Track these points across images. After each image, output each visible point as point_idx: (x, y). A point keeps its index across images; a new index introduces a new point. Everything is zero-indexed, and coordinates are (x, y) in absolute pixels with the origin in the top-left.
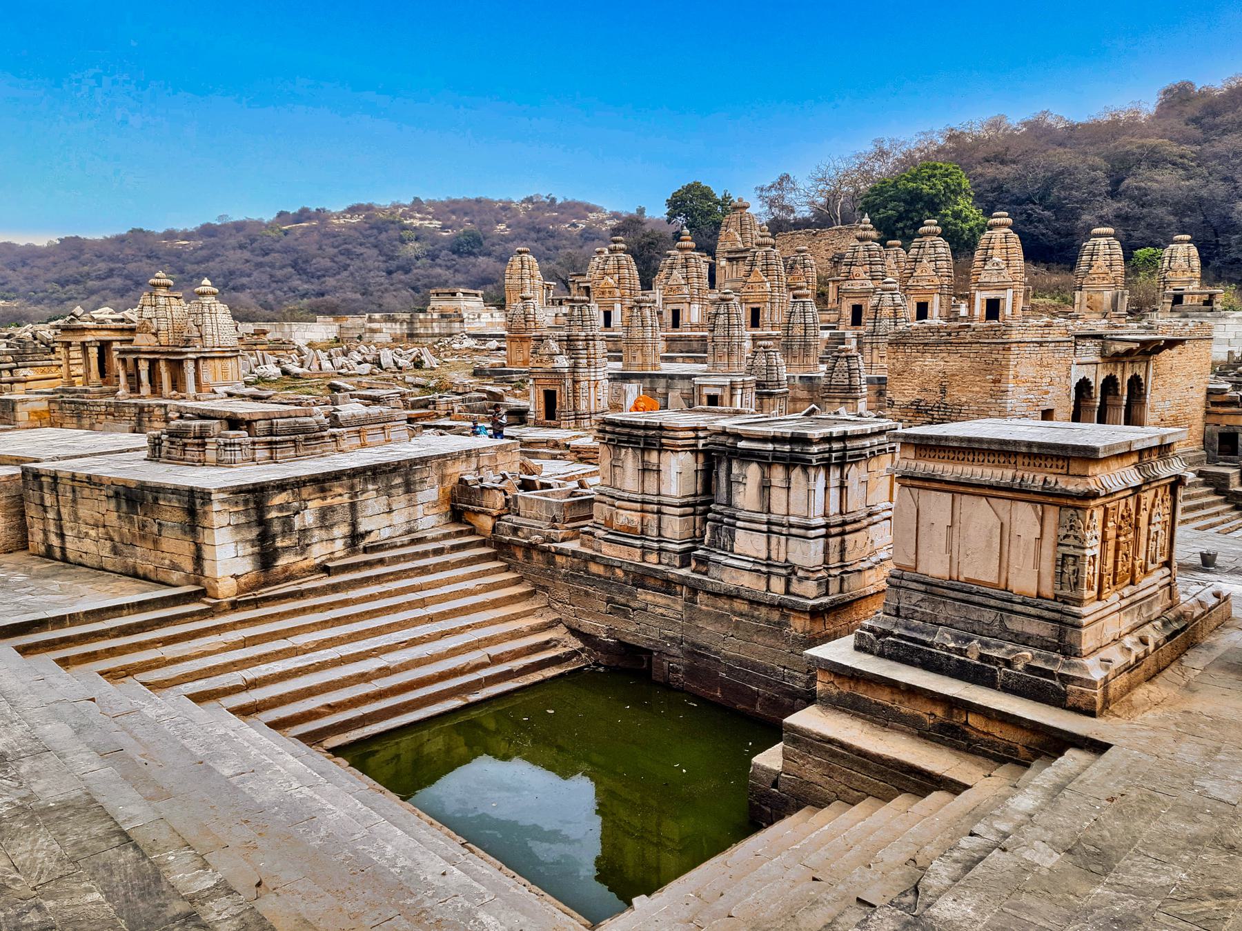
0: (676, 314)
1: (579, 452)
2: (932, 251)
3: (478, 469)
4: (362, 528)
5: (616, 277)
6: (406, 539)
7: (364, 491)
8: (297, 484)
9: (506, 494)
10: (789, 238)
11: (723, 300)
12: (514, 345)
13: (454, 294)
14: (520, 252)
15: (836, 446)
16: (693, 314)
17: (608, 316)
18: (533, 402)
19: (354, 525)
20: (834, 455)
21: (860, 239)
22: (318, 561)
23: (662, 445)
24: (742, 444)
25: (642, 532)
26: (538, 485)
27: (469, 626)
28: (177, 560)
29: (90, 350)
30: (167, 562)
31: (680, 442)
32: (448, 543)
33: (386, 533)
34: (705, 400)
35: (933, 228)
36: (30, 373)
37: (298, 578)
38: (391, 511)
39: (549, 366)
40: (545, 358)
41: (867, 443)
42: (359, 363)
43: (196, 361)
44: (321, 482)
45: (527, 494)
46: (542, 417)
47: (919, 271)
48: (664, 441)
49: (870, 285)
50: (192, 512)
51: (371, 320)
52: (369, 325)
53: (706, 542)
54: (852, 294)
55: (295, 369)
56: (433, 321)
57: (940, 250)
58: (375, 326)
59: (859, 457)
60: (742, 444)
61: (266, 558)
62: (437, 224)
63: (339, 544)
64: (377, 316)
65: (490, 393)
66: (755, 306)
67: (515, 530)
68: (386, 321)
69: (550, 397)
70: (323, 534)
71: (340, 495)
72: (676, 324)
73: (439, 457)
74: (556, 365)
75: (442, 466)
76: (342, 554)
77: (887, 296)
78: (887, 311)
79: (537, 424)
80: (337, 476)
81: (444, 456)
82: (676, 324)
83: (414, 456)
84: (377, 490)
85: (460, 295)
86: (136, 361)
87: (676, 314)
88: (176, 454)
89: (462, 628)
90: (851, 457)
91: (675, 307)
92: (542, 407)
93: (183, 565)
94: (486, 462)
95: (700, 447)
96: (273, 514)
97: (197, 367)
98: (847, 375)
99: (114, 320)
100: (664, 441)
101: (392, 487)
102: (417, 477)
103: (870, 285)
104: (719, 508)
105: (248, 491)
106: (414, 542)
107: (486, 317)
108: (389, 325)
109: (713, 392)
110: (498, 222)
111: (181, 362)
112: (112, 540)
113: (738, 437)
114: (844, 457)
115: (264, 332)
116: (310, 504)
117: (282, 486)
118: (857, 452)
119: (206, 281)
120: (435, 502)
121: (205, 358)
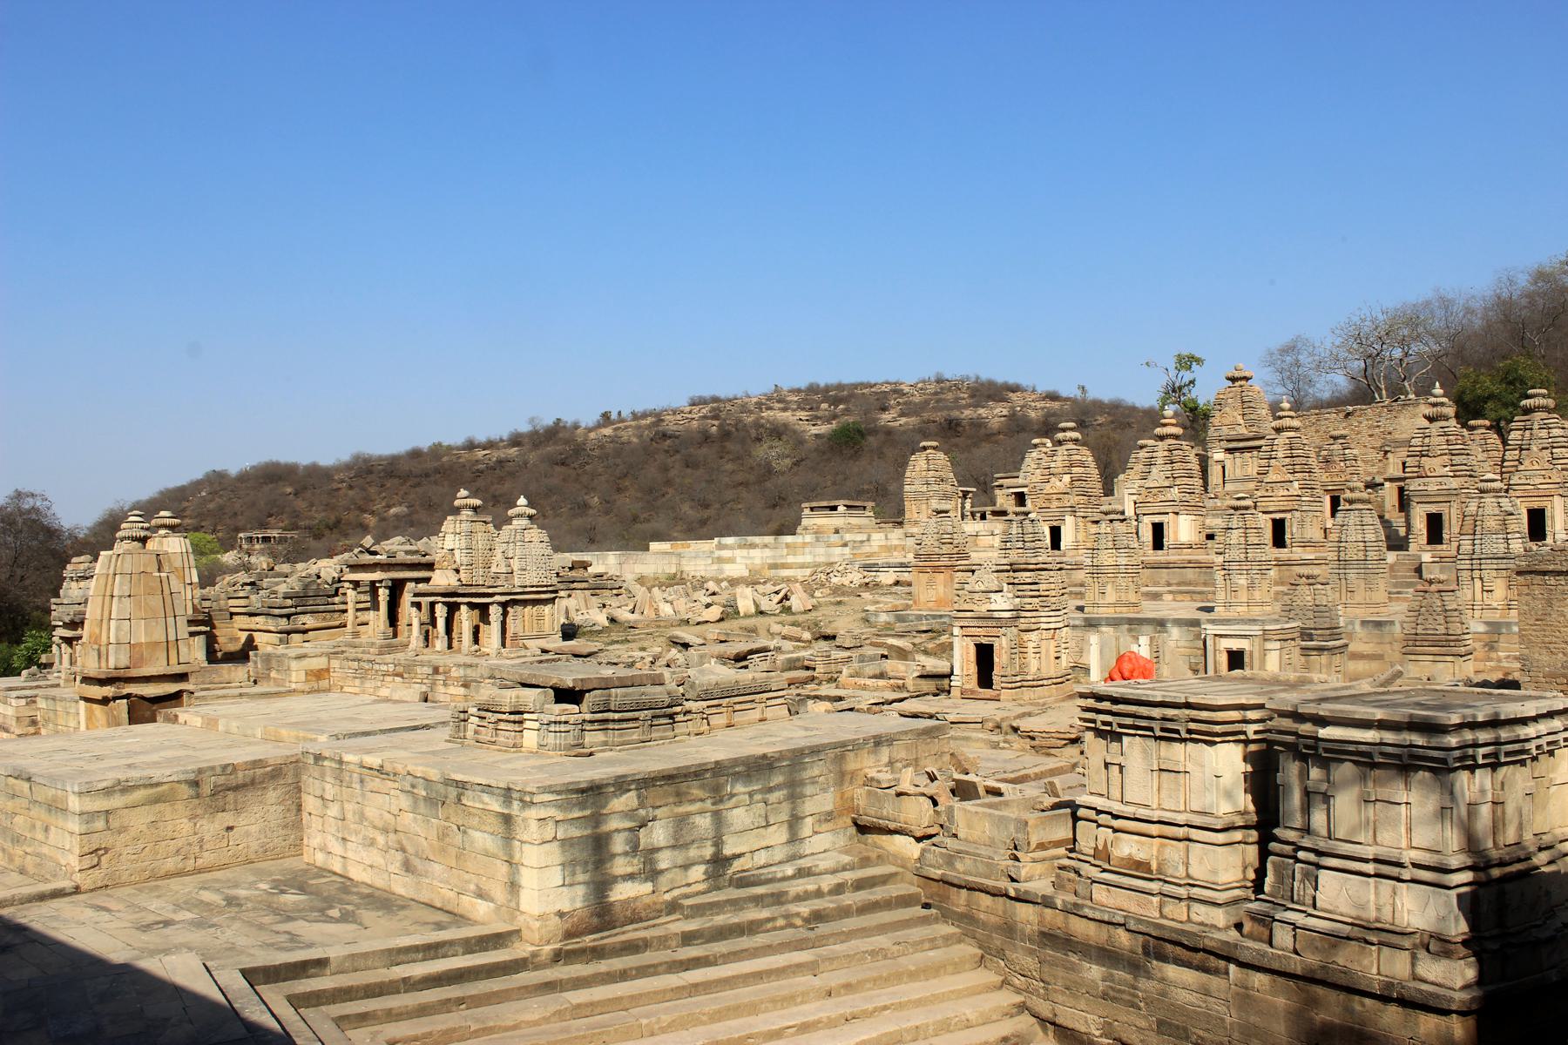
0: (1158, 529)
1: (1033, 738)
2: (1544, 433)
3: (891, 763)
4: (728, 851)
5: (1067, 478)
6: (790, 871)
7: (732, 795)
8: (646, 783)
9: (935, 803)
10: (1313, 419)
11: (1236, 509)
12: (924, 577)
13: (834, 508)
14: (925, 448)
15: (1484, 736)
16: (1183, 529)
17: (1056, 533)
18: (963, 662)
19: (718, 843)
20: (1482, 751)
21: (1431, 419)
22: (668, 897)
23: (1189, 731)
24: (1324, 733)
25: (1159, 871)
26: (981, 791)
27: (885, 1008)
29: (381, 591)
30: (472, 887)
31: (1218, 728)
32: (849, 876)
33: (761, 859)
34: (1223, 659)
35: (1543, 402)
36: (309, 621)
37: (641, 920)
38: (768, 825)
39: (984, 608)
40: (976, 596)
41: (1530, 731)
42: (708, 606)
43: (504, 605)
44: (674, 781)
45: (968, 805)
46: (973, 683)
47: (1527, 463)
48: (1192, 726)
49: (1454, 483)
50: (507, 819)
51: (721, 547)
52: (718, 553)
53: (1266, 889)
54: (1426, 499)
55: (624, 615)
56: (804, 545)
57: (1556, 432)
58: (725, 554)
59: (1520, 756)
60: (1324, 733)
61: (601, 887)
62: (803, 414)
63: (698, 872)
64: (730, 540)
65: (891, 647)
66: (1278, 516)
67: (950, 860)
68: (740, 547)
69: (985, 655)
70: (680, 857)
71: (702, 800)
72: (1158, 543)
73: (835, 746)
74: (993, 607)
75: (840, 759)
76: (702, 887)
77: (1489, 500)
78: (1492, 523)
79: (966, 695)
80: (695, 773)
81: (843, 744)
82: (1158, 543)
83: (802, 743)
84: (751, 794)
85: (841, 509)
86: (432, 604)
87: (1158, 529)
88: (486, 735)
89: (875, 1010)
90: (1507, 754)
91: (1157, 519)
92: (973, 669)
93: (492, 893)
94: (903, 755)
95: (1252, 737)
96: (613, 824)
97: (505, 614)
98: (1441, 619)
99: (407, 552)
100: (1192, 726)
101: (770, 790)
102: (806, 774)
103: (1454, 483)
104: (1291, 835)
105: (583, 791)
106: (802, 873)
107: (878, 538)
108: (744, 552)
109: (1235, 645)
110: (884, 409)
112: (403, 850)
113: (1322, 721)
114: (1495, 755)
115: (585, 566)
116: (658, 812)
117: (621, 784)
118: (1517, 747)
119: (522, 501)
120: (830, 813)
121: (515, 602)
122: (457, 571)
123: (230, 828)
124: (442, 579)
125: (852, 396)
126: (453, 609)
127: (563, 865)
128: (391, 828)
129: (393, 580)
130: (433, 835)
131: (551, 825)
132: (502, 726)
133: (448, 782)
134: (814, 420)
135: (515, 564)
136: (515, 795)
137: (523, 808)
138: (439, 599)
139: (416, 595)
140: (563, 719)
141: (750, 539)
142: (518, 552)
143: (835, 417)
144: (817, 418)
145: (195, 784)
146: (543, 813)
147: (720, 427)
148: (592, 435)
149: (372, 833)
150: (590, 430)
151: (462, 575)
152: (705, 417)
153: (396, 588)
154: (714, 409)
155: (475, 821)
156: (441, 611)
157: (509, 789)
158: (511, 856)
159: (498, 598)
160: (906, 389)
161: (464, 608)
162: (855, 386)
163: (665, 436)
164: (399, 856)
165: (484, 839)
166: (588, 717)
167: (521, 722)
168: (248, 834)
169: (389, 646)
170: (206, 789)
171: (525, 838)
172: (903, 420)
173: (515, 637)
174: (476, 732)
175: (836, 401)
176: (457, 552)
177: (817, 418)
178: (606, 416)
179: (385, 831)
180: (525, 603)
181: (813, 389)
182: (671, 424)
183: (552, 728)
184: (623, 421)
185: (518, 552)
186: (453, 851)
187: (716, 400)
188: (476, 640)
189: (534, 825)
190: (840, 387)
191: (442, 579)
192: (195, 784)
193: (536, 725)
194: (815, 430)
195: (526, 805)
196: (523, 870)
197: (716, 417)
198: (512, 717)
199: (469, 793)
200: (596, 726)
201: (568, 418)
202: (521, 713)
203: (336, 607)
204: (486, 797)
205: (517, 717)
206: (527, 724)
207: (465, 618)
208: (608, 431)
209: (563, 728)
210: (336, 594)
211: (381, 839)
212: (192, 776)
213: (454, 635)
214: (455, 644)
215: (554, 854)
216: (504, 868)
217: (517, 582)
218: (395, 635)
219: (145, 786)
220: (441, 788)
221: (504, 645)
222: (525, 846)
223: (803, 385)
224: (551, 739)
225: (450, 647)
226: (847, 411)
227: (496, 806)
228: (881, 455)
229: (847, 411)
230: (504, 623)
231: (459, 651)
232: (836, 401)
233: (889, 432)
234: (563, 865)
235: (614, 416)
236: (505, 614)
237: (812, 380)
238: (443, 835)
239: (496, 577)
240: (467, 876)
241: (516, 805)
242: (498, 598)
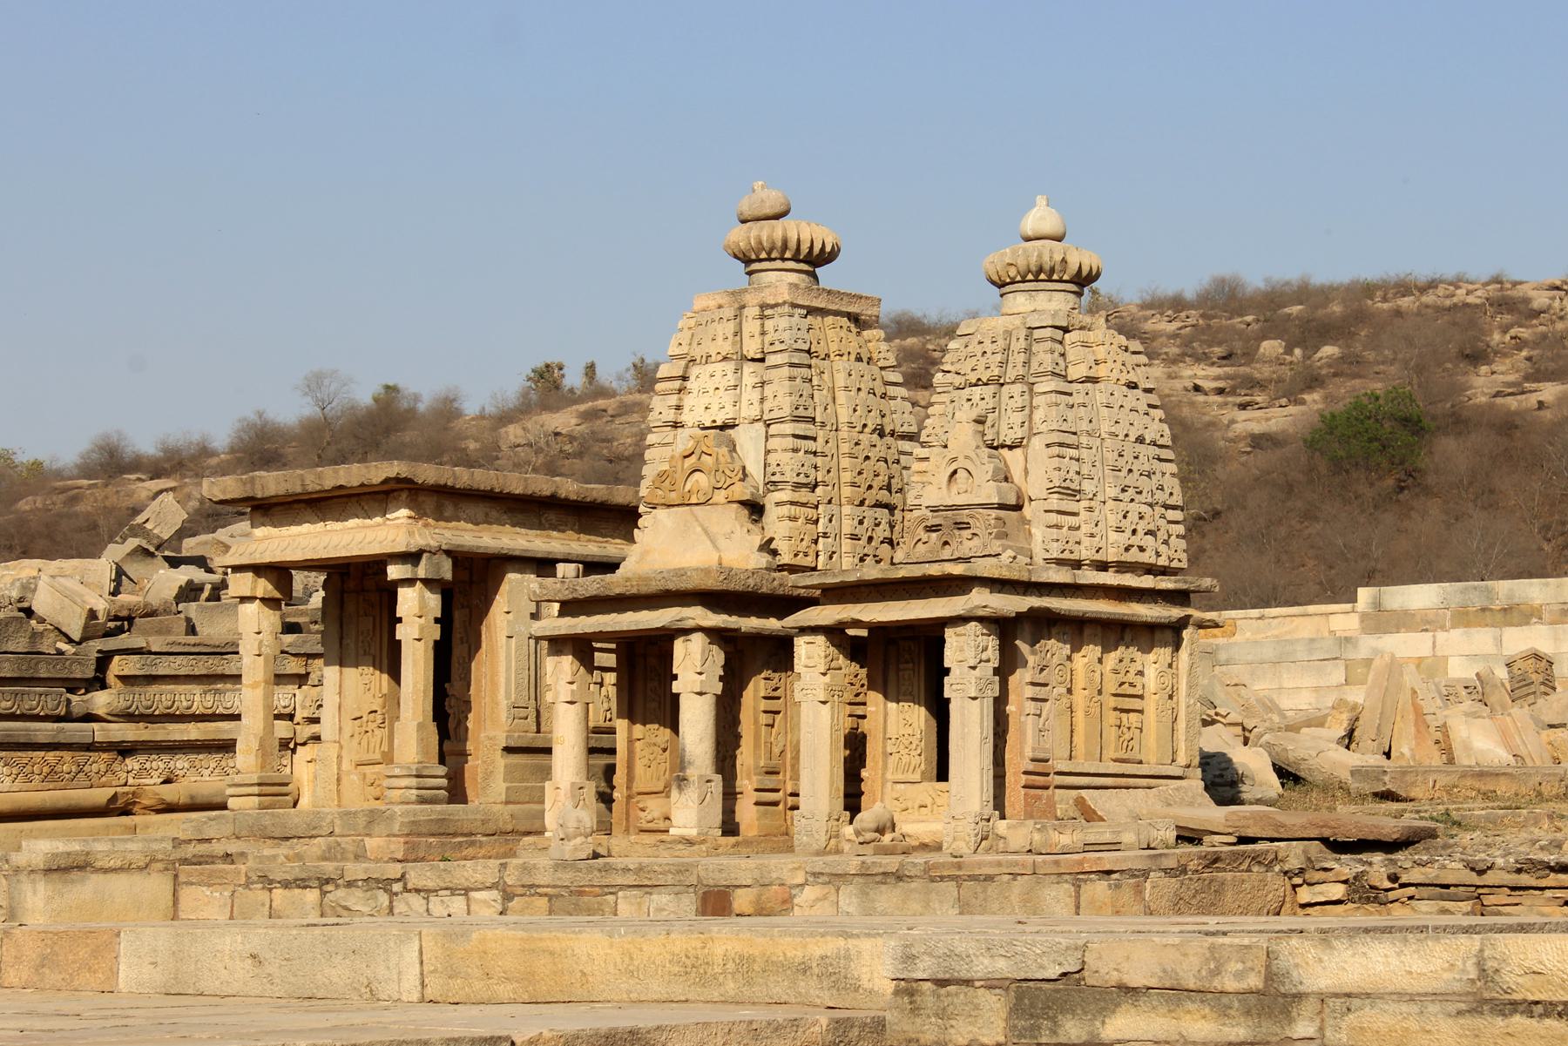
43: (1004, 628)
51: (1381, 621)
52: (1368, 644)
64: (1420, 596)
68: (1464, 618)
97: (1007, 665)
110: (1476, 356)
111: (929, 637)
121: (1043, 624)
122: (755, 509)
124: (667, 547)
125: (1360, 316)
126: (753, 658)
129: (462, 559)
134: (1242, 390)
135: (1036, 472)
139: (570, 607)
141: (1506, 589)
142: (1046, 415)
143: (1313, 381)
144: (1253, 384)
148: (513, 433)
150: (505, 418)
151: (777, 523)
153: (468, 587)
159: (980, 600)
160: (1540, 300)
161: (810, 653)
162: (1368, 290)
169: (443, 830)
172: (1549, 391)
173: (1040, 776)
175: (1312, 332)
176: (749, 441)
177: (1253, 384)
178: (547, 381)
180: (1077, 629)
181: (1224, 299)
184: (604, 393)
190: (1304, 293)
194: (1249, 423)
201: (422, 387)
203: (100, 732)
208: (564, 420)
210: (99, 682)
218: (457, 793)
223: (1190, 285)
225: (730, 827)
226: (1350, 365)
228: (1489, 499)
229: (1350, 365)
232: (1312, 332)
233: (1508, 426)
235: (573, 379)
237: (1225, 270)
242: (980, 600)
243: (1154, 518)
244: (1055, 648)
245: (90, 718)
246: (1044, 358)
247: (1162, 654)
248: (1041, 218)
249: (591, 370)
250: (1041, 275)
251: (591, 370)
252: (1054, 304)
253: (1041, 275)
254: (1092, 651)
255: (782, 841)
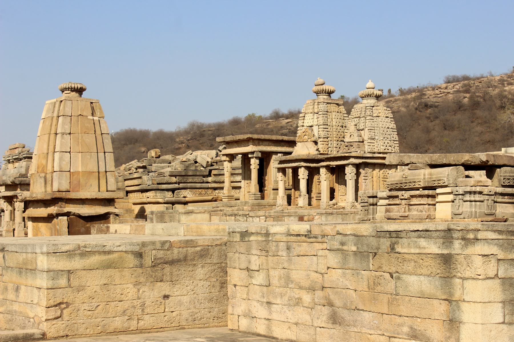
28: (420, 325)
29: (253, 161)
30: (406, 329)
36: (189, 195)
43: (358, 167)
50: (447, 260)
86: (295, 171)
97: (358, 174)
111: (343, 167)
112: (331, 304)
121: (366, 165)
122: (316, 143)
123: (166, 297)
124: (301, 150)
126: (313, 172)
127: (503, 302)
128: (319, 286)
129: (262, 152)
130: (363, 286)
131: (493, 261)
132: (415, 201)
133: (380, 234)
135: (366, 135)
136: (456, 235)
137: (466, 246)
138: (303, 164)
139: (281, 162)
140: (478, 189)
145: (139, 255)
146: (487, 249)
147: (471, 98)
149: (297, 293)
151: (320, 146)
152: (458, 91)
153: (265, 159)
154: (465, 85)
155: (410, 266)
156: (303, 174)
157: (449, 230)
158: (451, 294)
159: (352, 160)
161: (323, 171)
163: (427, 106)
164: (326, 310)
165: (417, 282)
166: (500, 190)
167: (433, 197)
168: (180, 303)
169: (259, 205)
170: (148, 261)
171: (468, 274)
174: (387, 211)
176: (315, 128)
179: (312, 289)
180: (374, 166)
182: (431, 97)
183: (467, 197)
184: (392, 96)
185: (368, 124)
186: (385, 298)
187: (466, 78)
188: (332, 197)
189: (478, 261)
191: (301, 150)
192: (139, 255)
193: (451, 197)
195: (467, 242)
196: (464, 306)
197: (467, 91)
198: (426, 192)
199: (404, 240)
200: (506, 199)
202: (434, 188)
203: (210, 185)
204: (423, 242)
205: (431, 192)
206: (440, 198)
207: (324, 179)
209: (477, 197)
210: (209, 175)
211: (307, 298)
212: (137, 248)
213: (313, 195)
214: (314, 202)
215: (493, 291)
216: (440, 309)
217: (367, 148)
218: (263, 198)
219: (100, 253)
220: (373, 242)
221: (356, 200)
222: (467, 283)
224: (466, 208)
225: (310, 204)
227: (434, 248)
230: (357, 182)
231: (318, 207)
234: (503, 302)
236: (358, 174)
238: (374, 285)
239: (350, 145)
240: (399, 320)
241: (457, 244)
242: (352, 160)
243: (391, 143)
244: (369, 170)
245: (208, 182)
246: (368, 113)
247: (393, 170)
248: (370, 84)
249: (389, 91)
250: (368, 96)
251: (389, 91)
252: (372, 101)
253: (368, 96)
254: (377, 170)
255: (318, 207)
